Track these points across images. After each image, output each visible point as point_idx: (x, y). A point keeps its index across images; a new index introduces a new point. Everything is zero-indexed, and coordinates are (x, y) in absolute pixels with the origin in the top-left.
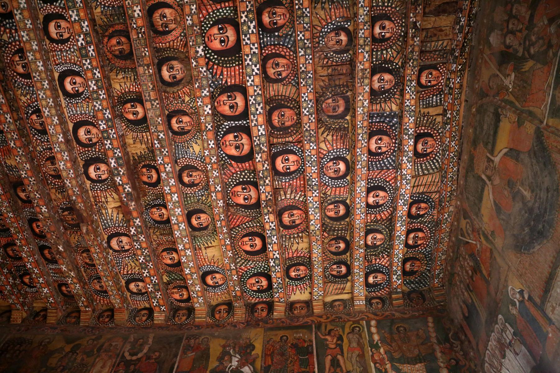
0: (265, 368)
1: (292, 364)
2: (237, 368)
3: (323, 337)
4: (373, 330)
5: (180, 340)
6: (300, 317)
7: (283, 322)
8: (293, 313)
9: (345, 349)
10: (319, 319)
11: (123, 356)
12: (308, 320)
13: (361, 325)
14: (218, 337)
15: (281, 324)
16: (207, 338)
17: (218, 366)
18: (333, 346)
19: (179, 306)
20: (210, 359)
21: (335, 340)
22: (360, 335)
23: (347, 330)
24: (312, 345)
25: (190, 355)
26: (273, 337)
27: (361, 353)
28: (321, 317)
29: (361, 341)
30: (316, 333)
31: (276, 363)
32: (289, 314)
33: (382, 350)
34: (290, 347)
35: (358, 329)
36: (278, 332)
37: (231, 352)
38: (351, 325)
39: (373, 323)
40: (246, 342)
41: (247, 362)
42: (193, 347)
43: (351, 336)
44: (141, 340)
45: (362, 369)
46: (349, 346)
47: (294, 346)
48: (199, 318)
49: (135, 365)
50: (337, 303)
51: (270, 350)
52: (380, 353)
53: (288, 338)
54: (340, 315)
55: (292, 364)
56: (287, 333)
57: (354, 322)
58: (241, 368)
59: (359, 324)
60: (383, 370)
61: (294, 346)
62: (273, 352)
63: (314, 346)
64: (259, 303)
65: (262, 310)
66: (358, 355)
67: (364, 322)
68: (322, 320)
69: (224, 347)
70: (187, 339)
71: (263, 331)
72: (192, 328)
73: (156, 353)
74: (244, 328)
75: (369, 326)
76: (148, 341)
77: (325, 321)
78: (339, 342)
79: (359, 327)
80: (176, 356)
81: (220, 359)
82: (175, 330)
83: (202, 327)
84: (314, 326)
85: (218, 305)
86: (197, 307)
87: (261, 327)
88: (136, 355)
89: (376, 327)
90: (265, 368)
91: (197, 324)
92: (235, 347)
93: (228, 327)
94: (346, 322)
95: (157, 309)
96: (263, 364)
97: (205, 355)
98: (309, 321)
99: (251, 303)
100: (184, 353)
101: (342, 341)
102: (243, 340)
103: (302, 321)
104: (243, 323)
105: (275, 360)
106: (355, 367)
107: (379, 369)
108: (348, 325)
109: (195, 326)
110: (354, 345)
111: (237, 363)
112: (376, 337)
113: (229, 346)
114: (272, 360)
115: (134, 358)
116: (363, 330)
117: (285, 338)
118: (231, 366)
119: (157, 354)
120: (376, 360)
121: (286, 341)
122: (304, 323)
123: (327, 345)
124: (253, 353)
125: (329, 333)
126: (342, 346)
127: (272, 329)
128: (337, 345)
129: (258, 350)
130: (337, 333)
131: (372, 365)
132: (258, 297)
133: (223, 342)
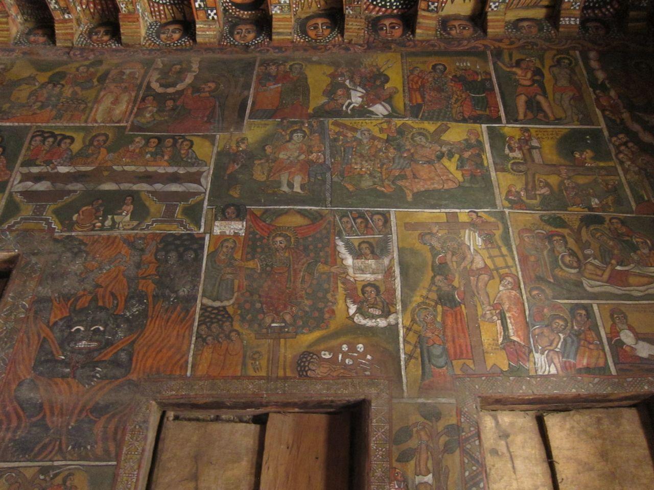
0: (411, 107)
1: (459, 104)
2: (361, 106)
3: (508, 70)
4: (594, 64)
5: (250, 65)
6: (463, 39)
7: (433, 45)
8: (449, 34)
9: (549, 87)
10: (497, 44)
11: (149, 87)
12: (479, 44)
13: (572, 56)
14: (319, 63)
15: (431, 48)
16: (300, 64)
17: (328, 103)
18: (528, 83)
19: (238, 17)
20: (312, 94)
21: (529, 75)
22: (573, 71)
23: (548, 62)
24: (491, 79)
25: (272, 87)
26: (419, 65)
27: (577, 95)
28: (500, 41)
29: (576, 78)
30: (494, 64)
31: (431, 101)
32: (441, 34)
33: (613, 93)
34: (452, 80)
35: (567, 61)
36: (425, 59)
37: (347, 82)
38: (555, 56)
39: (592, 55)
40: (372, 71)
41: (379, 99)
42: (275, 77)
43: (556, 70)
44: (178, 67)
45: (581, 116)
46: (556, 84)
47: (458, 79)
48: (279, 34)
49: (174, 100)
50: (525, 24)
51: (417, 82)
52: (610, 97)
53: (445, 68)
54: (533, 40)
55: (459, 104)
56: (444, 60)
57: (559, 52)
58: (369, 106)
59: (568, 54)
60: (618, 121)
61: (458, 79)
62: (423, 85)
63: (494, 80)
64: (385, 17)
65: (393, 28)
66: (573, 98)
67: (577, 53)
68: (502, 45)
69: (333, 76)
70: (261, 65)
71: (400, 57)
72: (268, 50)
73: (209, 84)
74: (365, 51)
75: (586, 59)
76: (191, 67)
77: (509, 47)
78: (536, 78)
79: (569, 59)
80: (247, 86)
81: (330, 92)
82: (237, 52)
83: (286, 50)
84: (489, 52)
85: (308, 19)
86: (276, 14)
87: (395, 51)
88: (174, 85)
89: (599, 60)
90: (411, 107)
91: (276, 45)
92: (352, 77)
93: (335, 50)
94: (546, 50)
95: (201, 14)
96: (407, 102)
97: (301, 88)
98: (480, 46)
99: (370, 17)
100: (260, 82)
101: (542, 75)
102: (365, 67)
103: (465, 46)
104: (361, 45)
105: (427, 96)
106: (569, 113)
107: (610, 119)
108: (548, 55)
109: (275, 48)
110: (563, 82)
111: (360, 100)
112: (601, 75)
113: (342, 75)
114: (423, 97)
115: (171, 90)
116: (577, 64)
117: (441, 67)
118: (350, 104)
119: (213, 85)
120: (605, 106)
121: (443, 72)
122: (471, 48)
123: (517, 81)
124: (387, 86)
125: (518, 64)
126: (543, 83)
127: (415, 54)
128: (534, 82)
129: (396, 80)
130: (531, 64)
131: (598, 112)
132: (385, 6)
133: (331, 70)
